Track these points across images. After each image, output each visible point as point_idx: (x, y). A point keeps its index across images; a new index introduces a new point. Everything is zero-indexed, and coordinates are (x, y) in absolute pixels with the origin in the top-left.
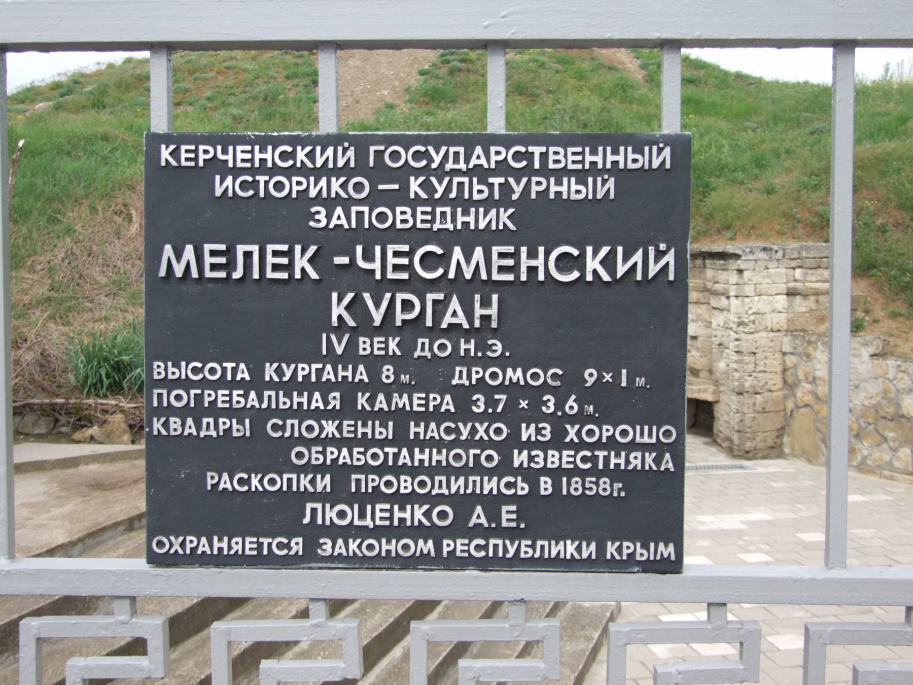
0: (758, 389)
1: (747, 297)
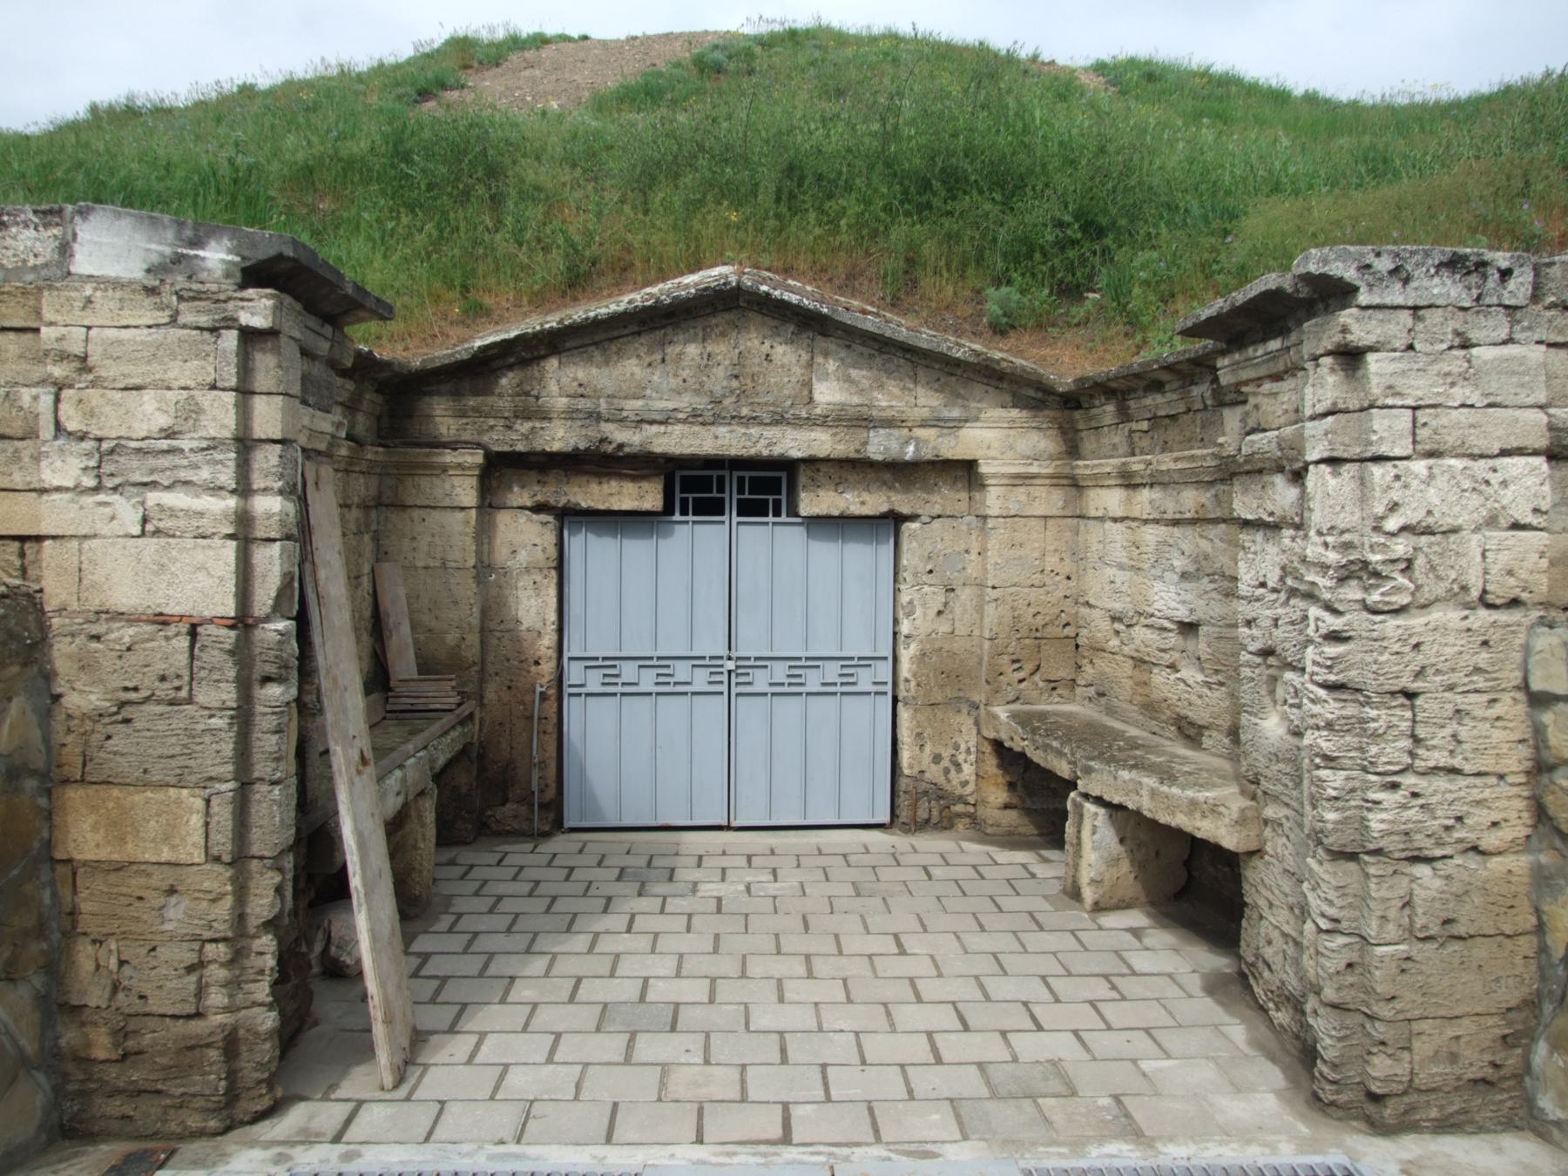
0: (1420, 840)
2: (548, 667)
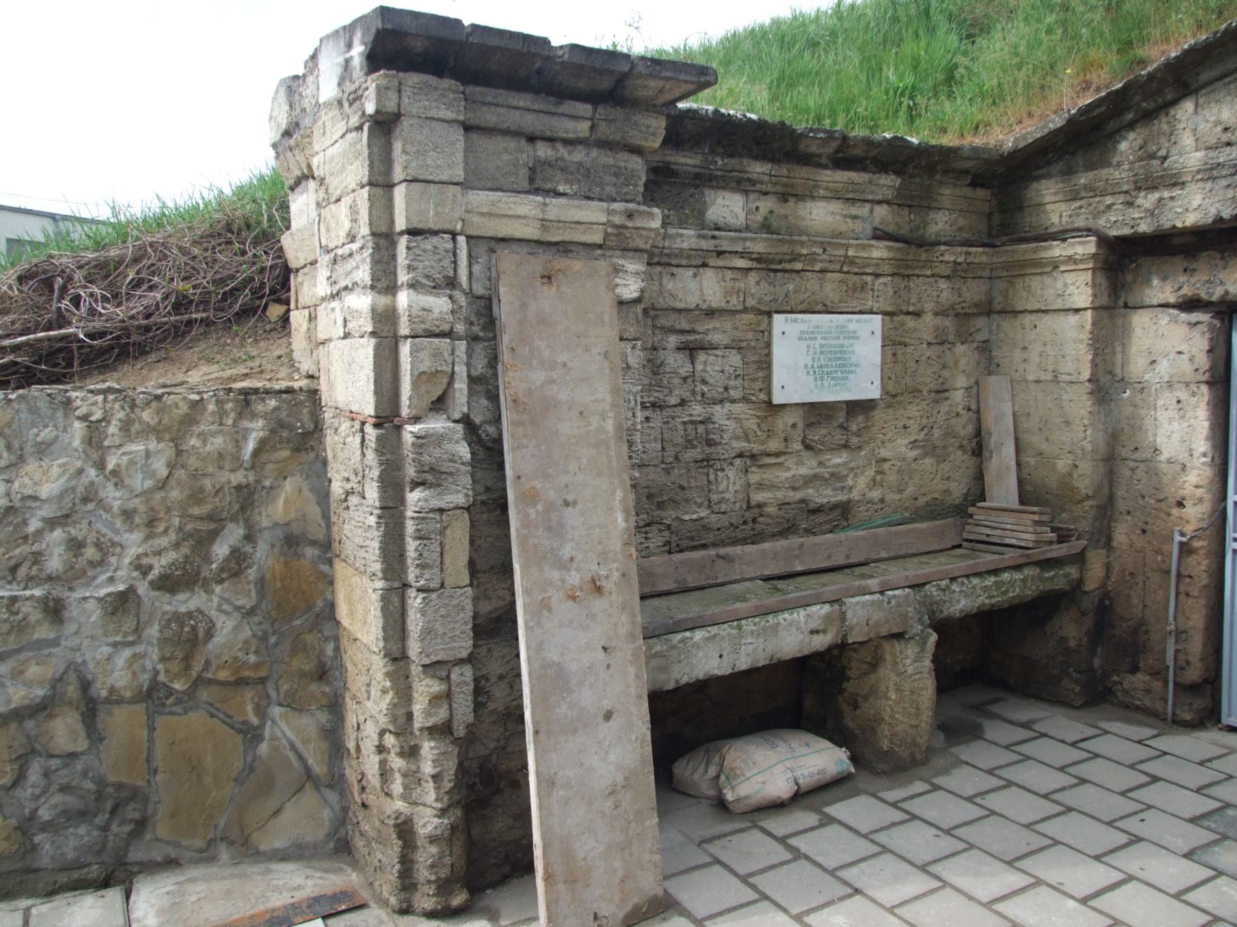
2: (1195, 514)
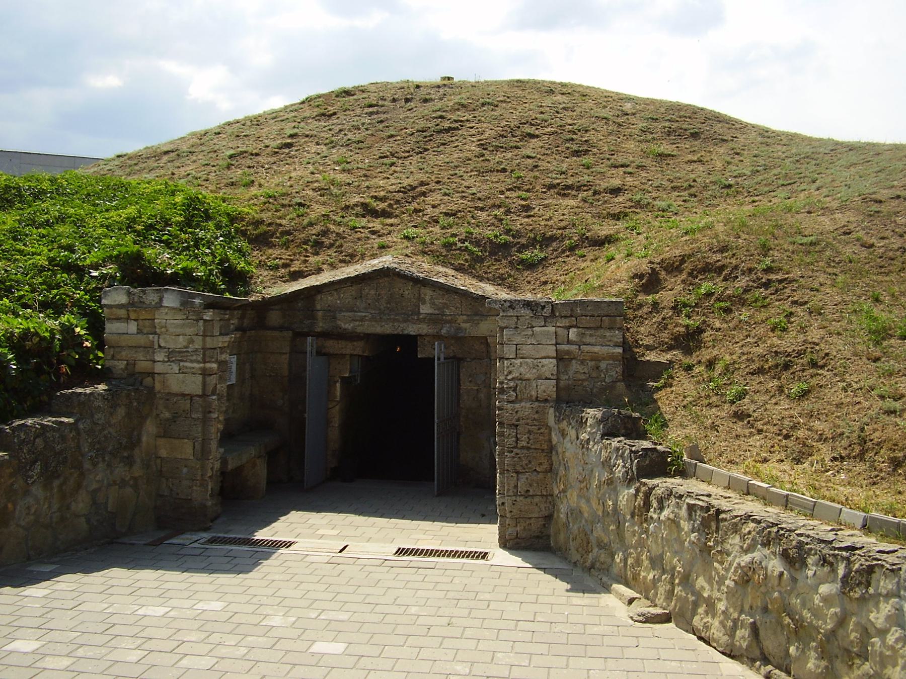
0: (519, 468)
1: (507, 359)
